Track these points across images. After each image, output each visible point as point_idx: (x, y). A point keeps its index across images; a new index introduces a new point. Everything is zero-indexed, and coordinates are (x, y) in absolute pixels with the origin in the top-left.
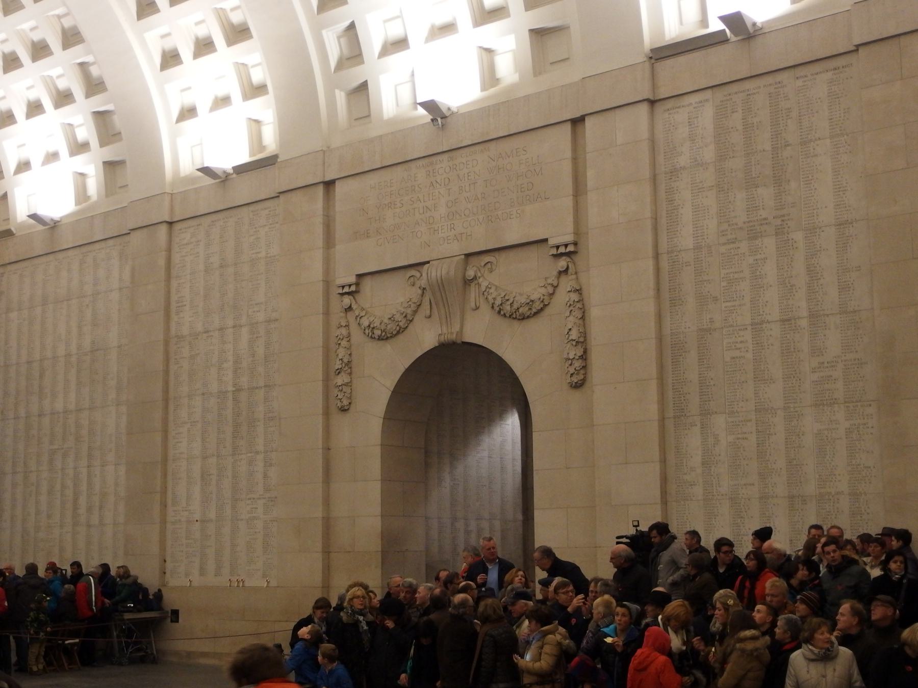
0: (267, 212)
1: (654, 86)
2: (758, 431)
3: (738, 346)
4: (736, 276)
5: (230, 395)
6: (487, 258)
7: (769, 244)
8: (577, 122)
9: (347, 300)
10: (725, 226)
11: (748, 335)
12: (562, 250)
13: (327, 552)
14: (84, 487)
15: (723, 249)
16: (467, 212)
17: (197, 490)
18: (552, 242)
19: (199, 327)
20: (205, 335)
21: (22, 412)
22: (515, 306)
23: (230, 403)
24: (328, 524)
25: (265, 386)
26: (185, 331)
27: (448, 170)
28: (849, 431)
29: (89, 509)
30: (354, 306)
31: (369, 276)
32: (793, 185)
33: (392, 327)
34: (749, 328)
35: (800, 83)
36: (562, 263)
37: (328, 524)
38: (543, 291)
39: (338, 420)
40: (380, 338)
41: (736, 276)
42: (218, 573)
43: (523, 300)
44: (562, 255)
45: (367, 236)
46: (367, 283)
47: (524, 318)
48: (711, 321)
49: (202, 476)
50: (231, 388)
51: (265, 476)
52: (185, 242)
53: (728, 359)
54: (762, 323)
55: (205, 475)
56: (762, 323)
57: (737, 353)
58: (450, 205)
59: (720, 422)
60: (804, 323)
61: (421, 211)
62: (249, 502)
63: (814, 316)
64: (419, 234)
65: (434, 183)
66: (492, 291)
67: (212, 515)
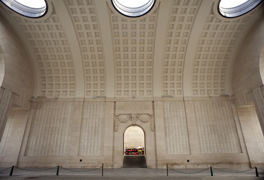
7: (176, 118)
8: (153, 102)
9: (117, 117)
13: (113, 151)
14: (59, 139)
19: (88, 117)
21: (44, 126)
23: (94, 129)
25: (101, 127)
26: (85, 117)
29: (60, 143)
33: (125, 121)
36: (151, 117)
39: (115, 132)
40: (123, 123)
42: (90, 154)
45: (121, 109)
46: (121, 115)
51: (101, 139)
55: (88, 139)
59: (171, 136)
63: (181, 126)
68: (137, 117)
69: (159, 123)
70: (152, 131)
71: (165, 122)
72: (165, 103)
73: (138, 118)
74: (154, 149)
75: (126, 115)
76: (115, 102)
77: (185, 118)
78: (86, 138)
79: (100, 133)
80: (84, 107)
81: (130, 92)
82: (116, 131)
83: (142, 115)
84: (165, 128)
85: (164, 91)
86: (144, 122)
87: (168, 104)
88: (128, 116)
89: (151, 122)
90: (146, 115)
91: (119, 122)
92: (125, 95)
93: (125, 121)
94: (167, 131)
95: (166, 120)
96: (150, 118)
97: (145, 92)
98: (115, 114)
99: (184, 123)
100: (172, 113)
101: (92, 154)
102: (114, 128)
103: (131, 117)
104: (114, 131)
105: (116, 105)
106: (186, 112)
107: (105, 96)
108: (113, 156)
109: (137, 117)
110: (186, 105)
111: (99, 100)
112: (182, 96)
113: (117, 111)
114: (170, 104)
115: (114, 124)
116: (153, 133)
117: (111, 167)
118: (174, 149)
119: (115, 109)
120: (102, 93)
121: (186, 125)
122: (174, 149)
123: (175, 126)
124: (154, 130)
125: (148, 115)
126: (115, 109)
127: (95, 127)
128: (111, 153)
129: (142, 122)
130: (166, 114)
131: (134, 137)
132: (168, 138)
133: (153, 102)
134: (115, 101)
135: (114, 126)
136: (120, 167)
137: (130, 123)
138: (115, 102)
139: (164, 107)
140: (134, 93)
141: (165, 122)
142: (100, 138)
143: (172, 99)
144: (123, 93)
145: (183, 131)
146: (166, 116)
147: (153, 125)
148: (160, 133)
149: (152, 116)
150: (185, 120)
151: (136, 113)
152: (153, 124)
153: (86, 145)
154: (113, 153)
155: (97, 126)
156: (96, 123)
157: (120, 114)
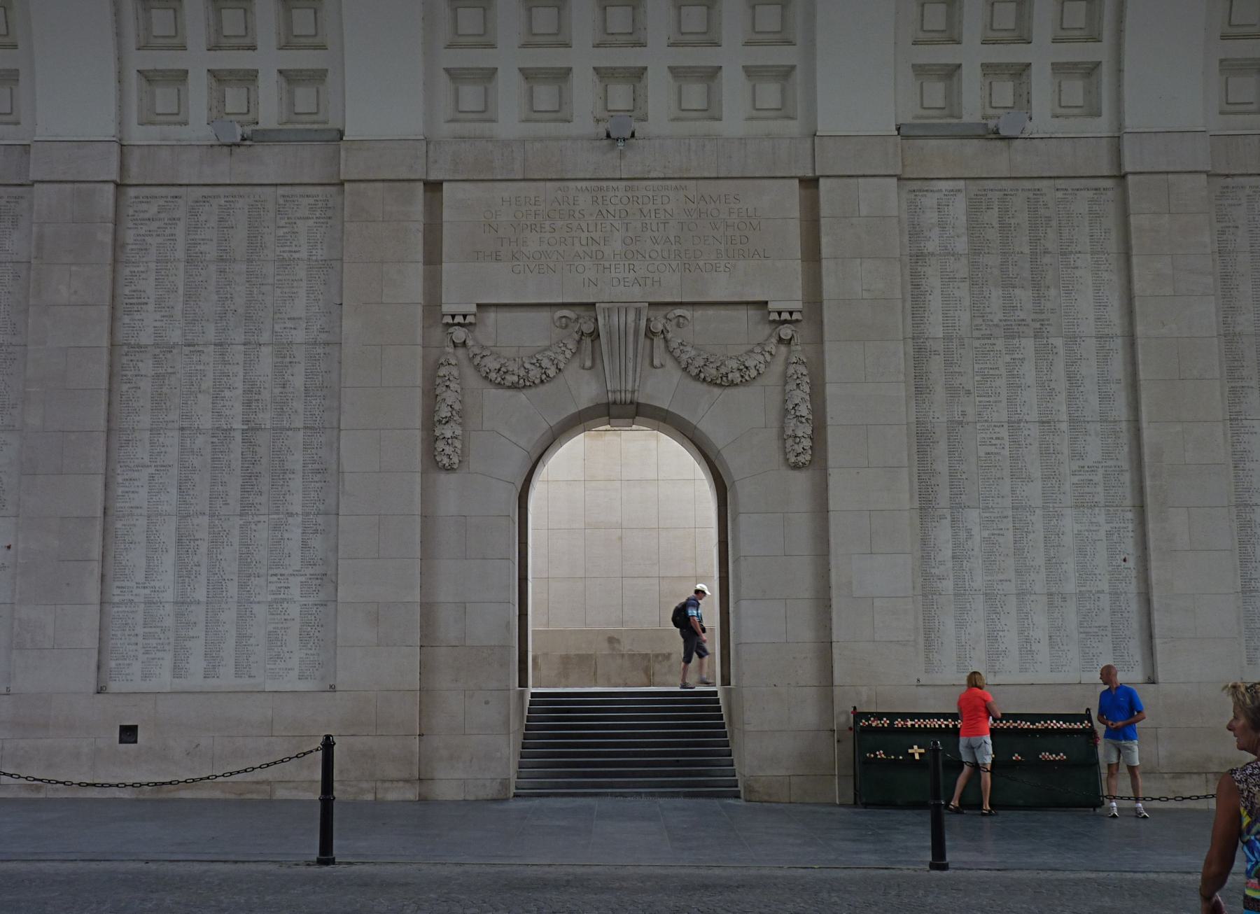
0: (311, 201)
1: (1120, 165)
2: (1015, 528)
3: (994, 442)
4: (992, 372)
5: (238, 437)
6: (679, 312)
7: (1028, 345)
8: (810, 183)
9: (459, 334)
10: (979, 321)
11: (1004, 433)
12: (785, 316)
15: (977, 343)
16: (654, 255)
17: (168, 560)
18: (771, 306)
19: (175, 336)
20: (186, 350)
22: (723, 370)
24: (428, 610)
25: (305, 428)
26: (146, 338)
27: (625, 200)
28: (1109, 534)
30: (470, 343)
31: (493, 309)
32: (1053, 292)
33: (535, 373)
34: (1006, 425)
35: (1060, 194)
36: (786, 331)
37: (428, 610)
38: (761, 358)
40: (514, 386)
41: (992, 372)
43: (734, 364)
44: (785, 322)
46: (491, 316)
47: (732, 384)
48: (964, 414)
49: (179, 541)
50: (238, 425)
51: (305, 545)
52: (147, 216)
53: (982, 454)
54: (1019, 421)
56: (1019, 421)
57: (993, 449)
58: (628, 241)
59: (973, 516)
60: (1064, 426)
61: (584, 242)
62: (275, 579)
63: (1075, 422)
64: (580, 269)
65: (604, 212)
66: (689, 349)
67: (201, 594)
68: (650, 334)
69: (863, 386)
70: (796, 467)
71: (920, 389)
72: (930, 201)
73: (659, 342)
74: (806, 634)
75: (545, 315)
76: (433, 187)
77: (1118, 344)
78: (168, 531)
79: (296, 483)
80: (130, 236)
81: (584, 93)
82: (450, 469)
83: (699, 313)
84: (922, 438)
85: (921, 71)
86: (722, 382)
87: (959, 209)
88: (565, 324)
89: (785, 379)
90: (742, 314)
91: (473, 380)
92: (533, 114)
93: (535, 373)
94: (942, 467)
95: (936, 366)
96: (780, 340)
97: (733, 86)
98: (432, 305)
99: (1104, 397)
100: (995, 296)
101: (227, 678)
102: (431, 440)
103: (595, 335)
104: (434, 462)
105: (447, 215)
106: (1137, 286)
107: (334, 124)
108: (426, 693)
109: (650, 334)
110: (1133, 220)
111: (269, 164)
112: (1102, 126)
113: (448, 268)
114: (975, 207)
115: (431, 397)
116: (801, 482)
117: (411, 794)
118: (993, 637)
119: (433, 256)
120: (304, 97)
121: (1120, 409)
122: (993, 637)
123: (1014, 424)
124: (810, 453)
125: (753, 313)
126: (433, 256)
127: (251, 429)
128: (402, 665)
129: (697, 378)
130: (935, 302)
131: (620, 520)
132: (943, 534)
133: (810, 183)
134: (433, 176)
135: (431, 423)
136: (490, 791)
137: (586, 391)
138: (433, 187)
139: (916, 233)
140: (620, 96)
141: (920, 389)
142: (295, 534)
143: (999, 160)
144: (509, 88)
145: (1093, 470)
146: (936, 330)
147: (804, 410)
148: (865, 483)
149: (799, 327)
150: (1117, 366)
151: (637, 294)
152: (800, 396)
153: (169, 596)
154: (426, 668)
155: (266, 418)
156: (251, 390)
157: (479, 306)
